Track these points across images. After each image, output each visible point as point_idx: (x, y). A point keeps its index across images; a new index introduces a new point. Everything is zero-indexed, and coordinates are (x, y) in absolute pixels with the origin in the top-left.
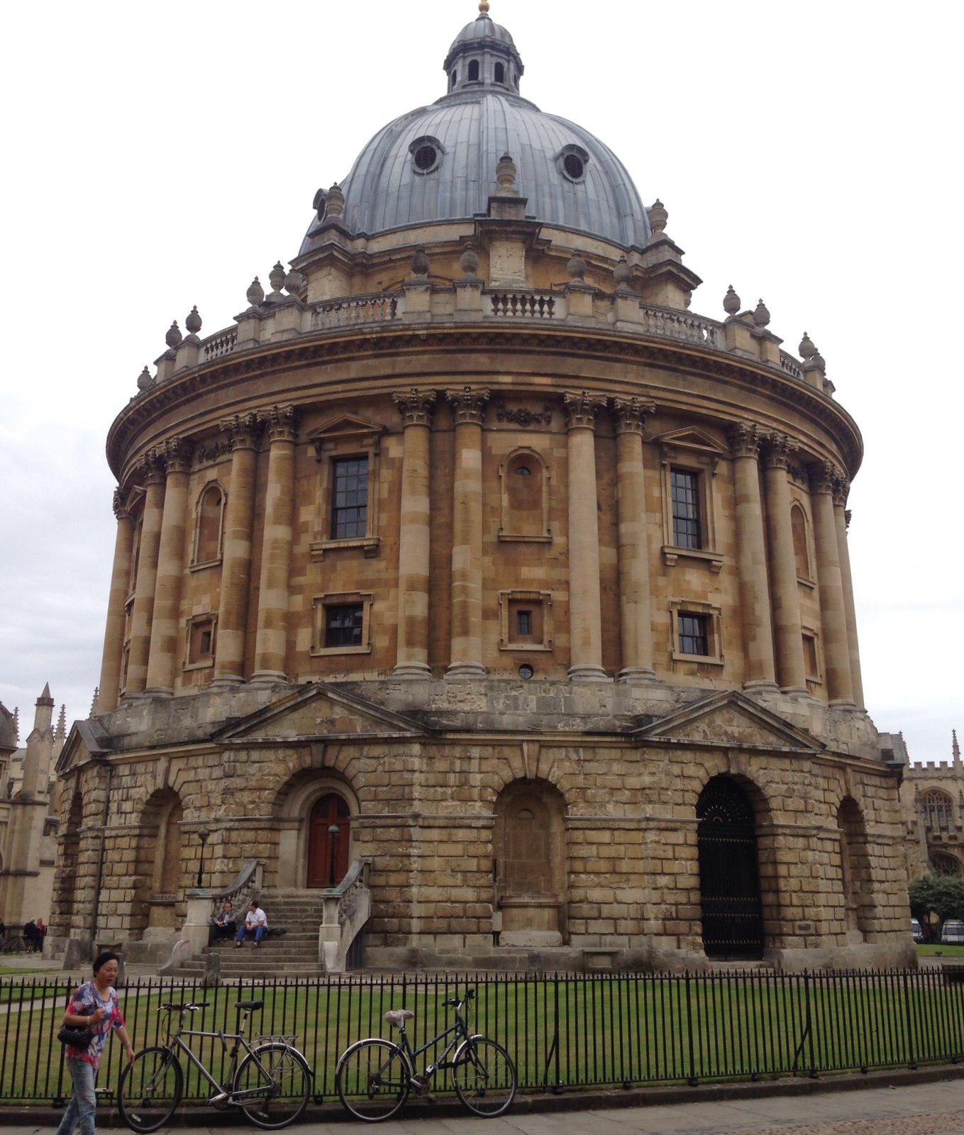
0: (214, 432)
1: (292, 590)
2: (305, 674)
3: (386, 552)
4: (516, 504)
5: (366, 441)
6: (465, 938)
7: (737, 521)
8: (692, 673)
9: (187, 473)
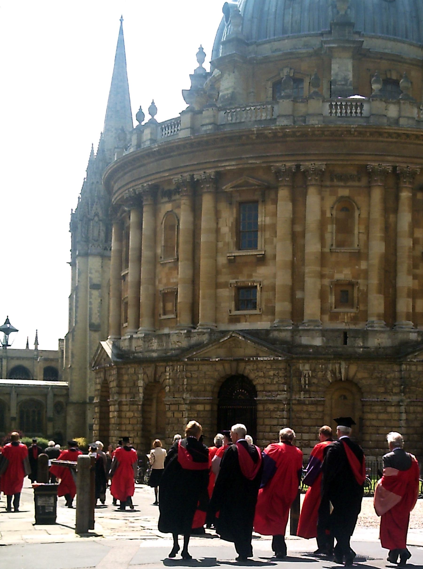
1: (415, 277)
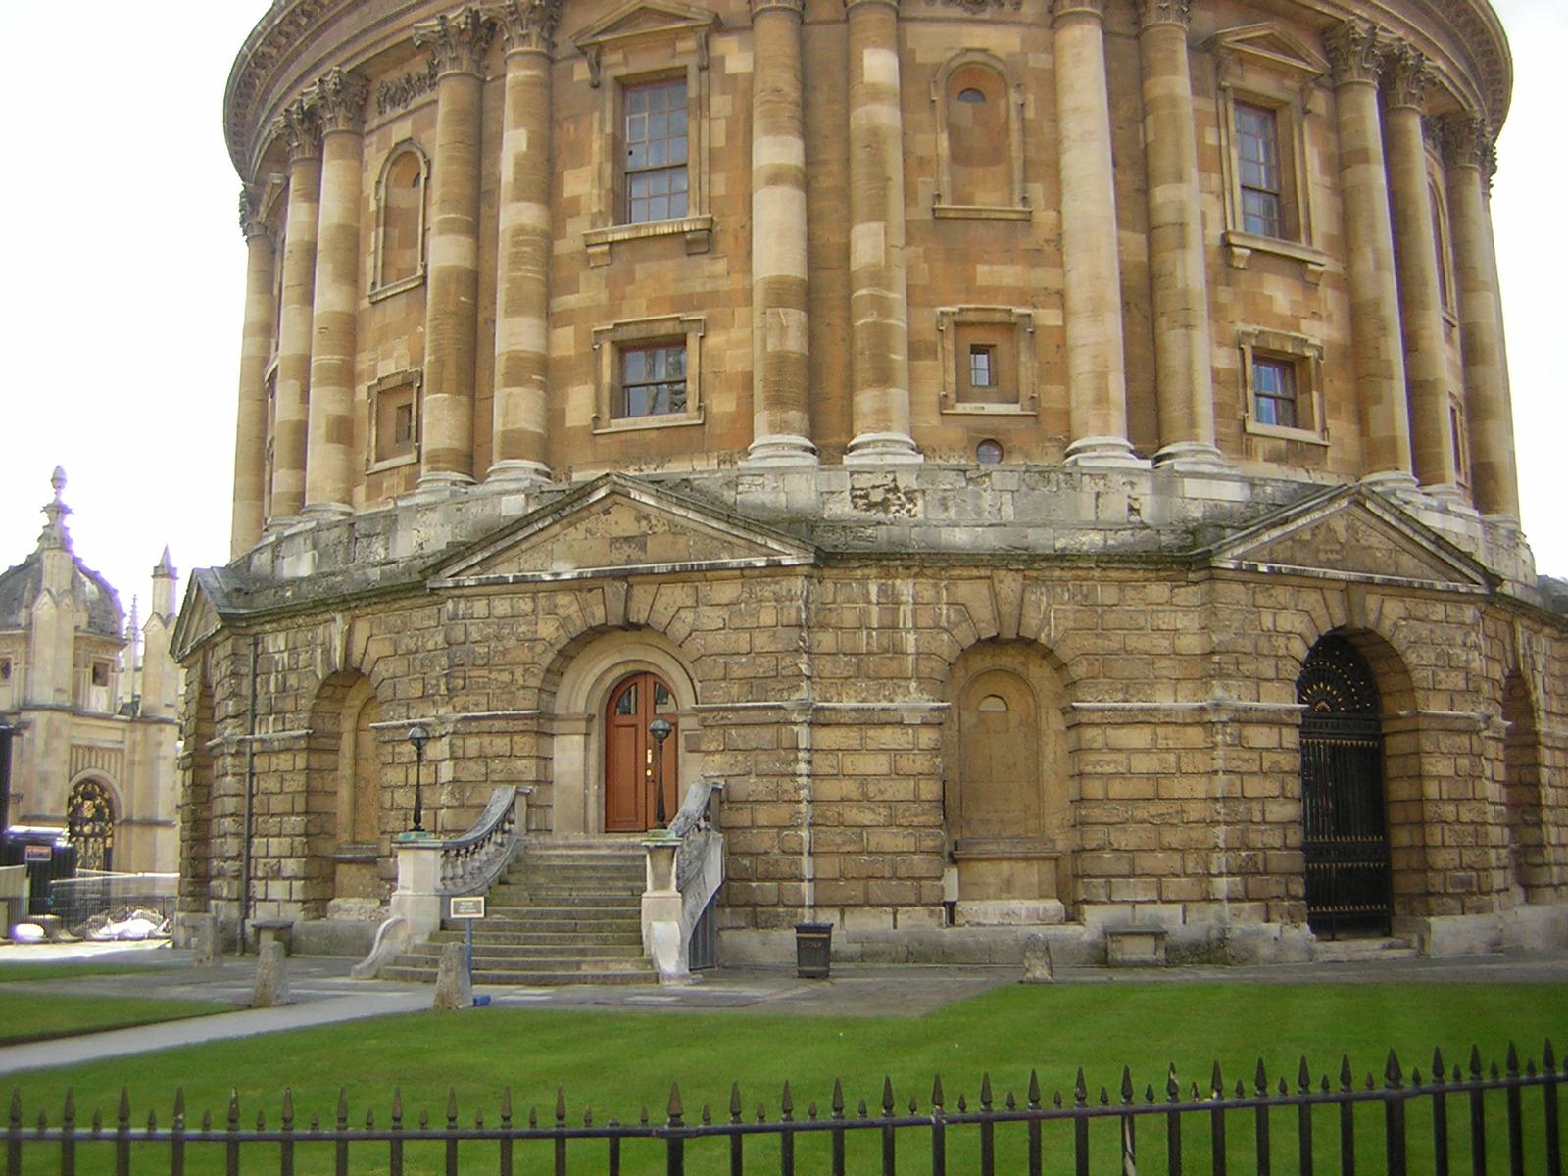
0: (404, 51)
2: (583, 467)
3: (726, 242)
4: (961, 155)
5: (681, 46)
6: (895, 914)
7: (1346, 200)
8: (1276, 457)
9: (358, 132)
